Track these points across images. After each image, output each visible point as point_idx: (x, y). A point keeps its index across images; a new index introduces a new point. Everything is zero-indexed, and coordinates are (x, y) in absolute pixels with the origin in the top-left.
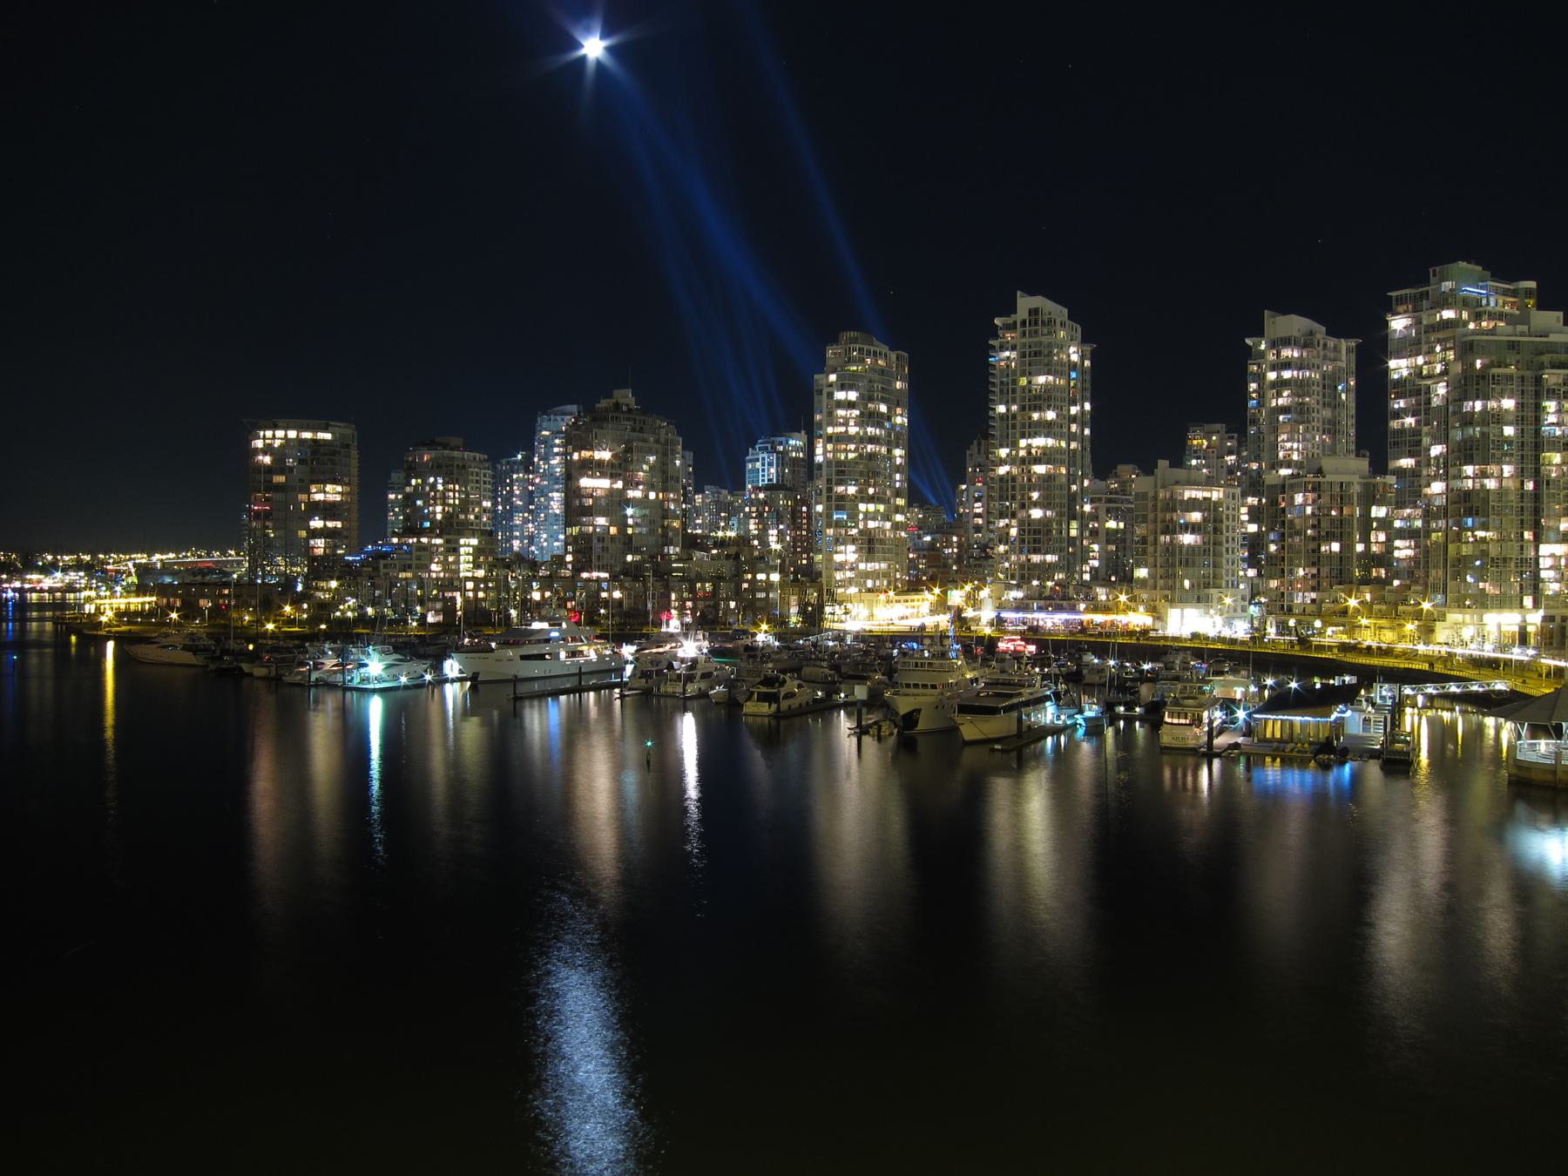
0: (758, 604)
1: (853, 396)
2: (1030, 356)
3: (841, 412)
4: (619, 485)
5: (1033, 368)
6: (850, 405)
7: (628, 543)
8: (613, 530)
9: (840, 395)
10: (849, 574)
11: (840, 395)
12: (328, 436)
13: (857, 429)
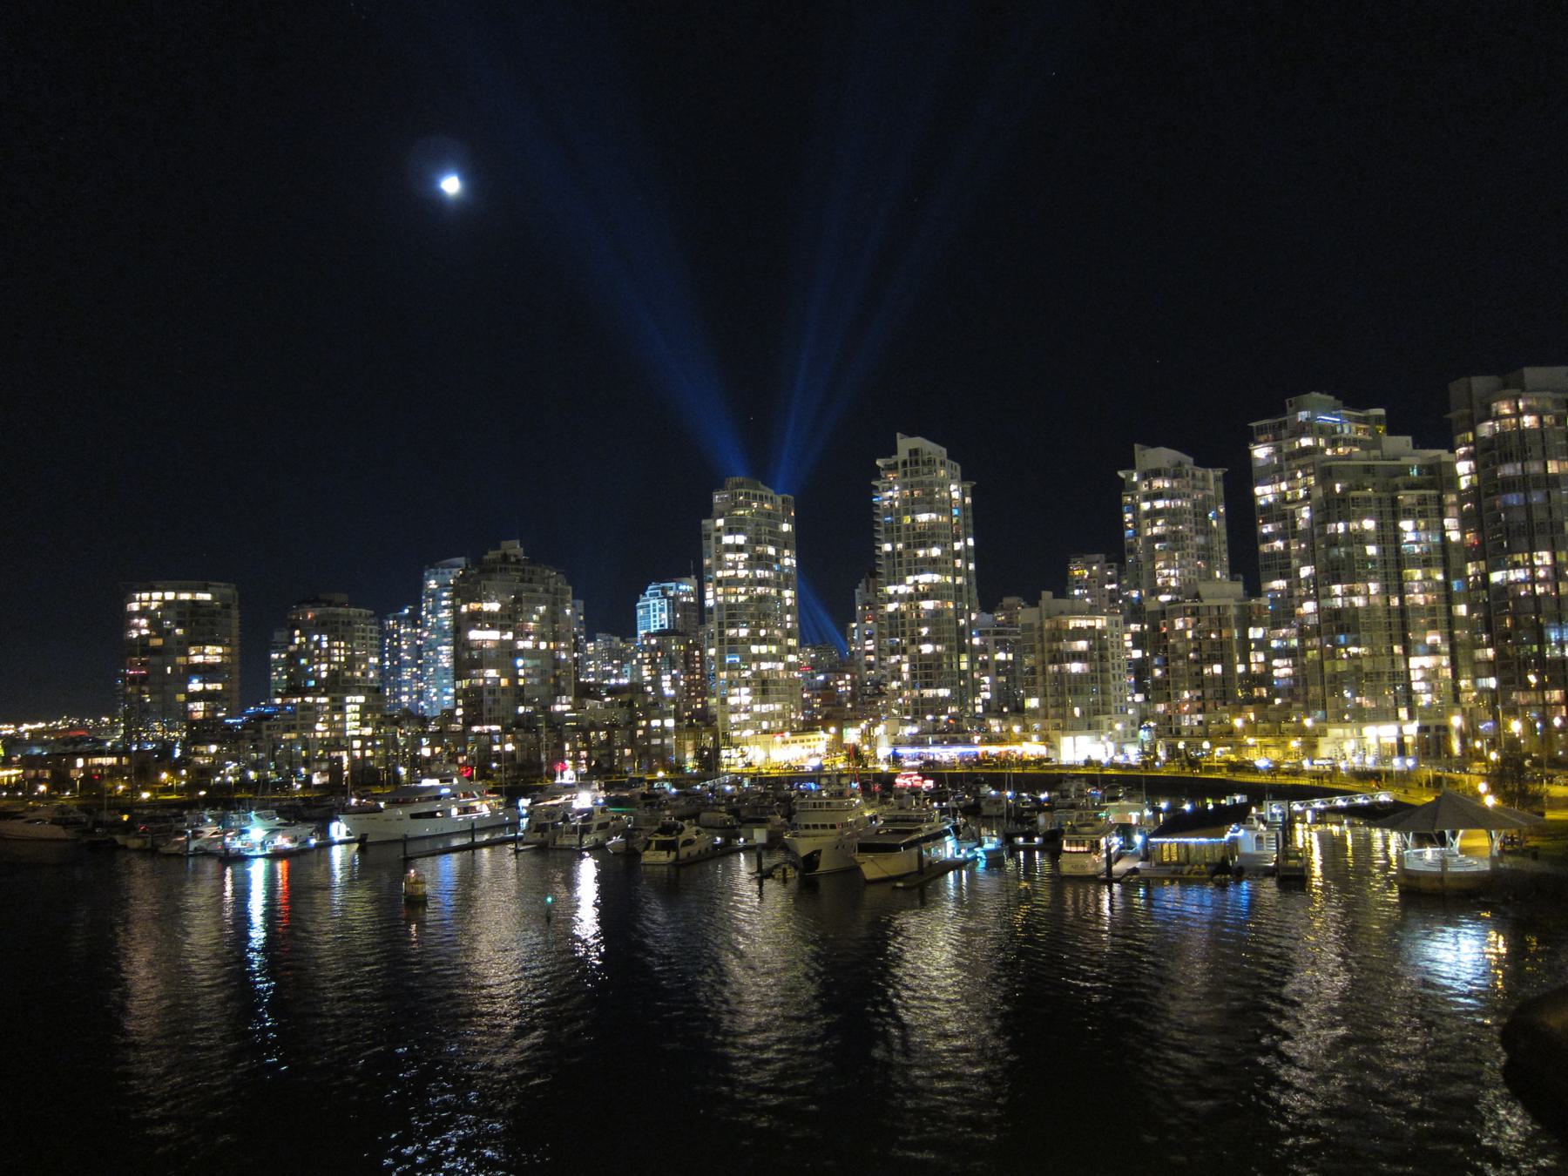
0: (653, 751)
1: (740, 539)
3: (729, 556)
4: (509, 636)
5: (916, 507)
6: (739, 549)
7: (519, 695)
8: (504, 682)
9: (728, 540)
10: (745, 717)
11: (728, 540)
12: (207, 597)
13: (746, 572)
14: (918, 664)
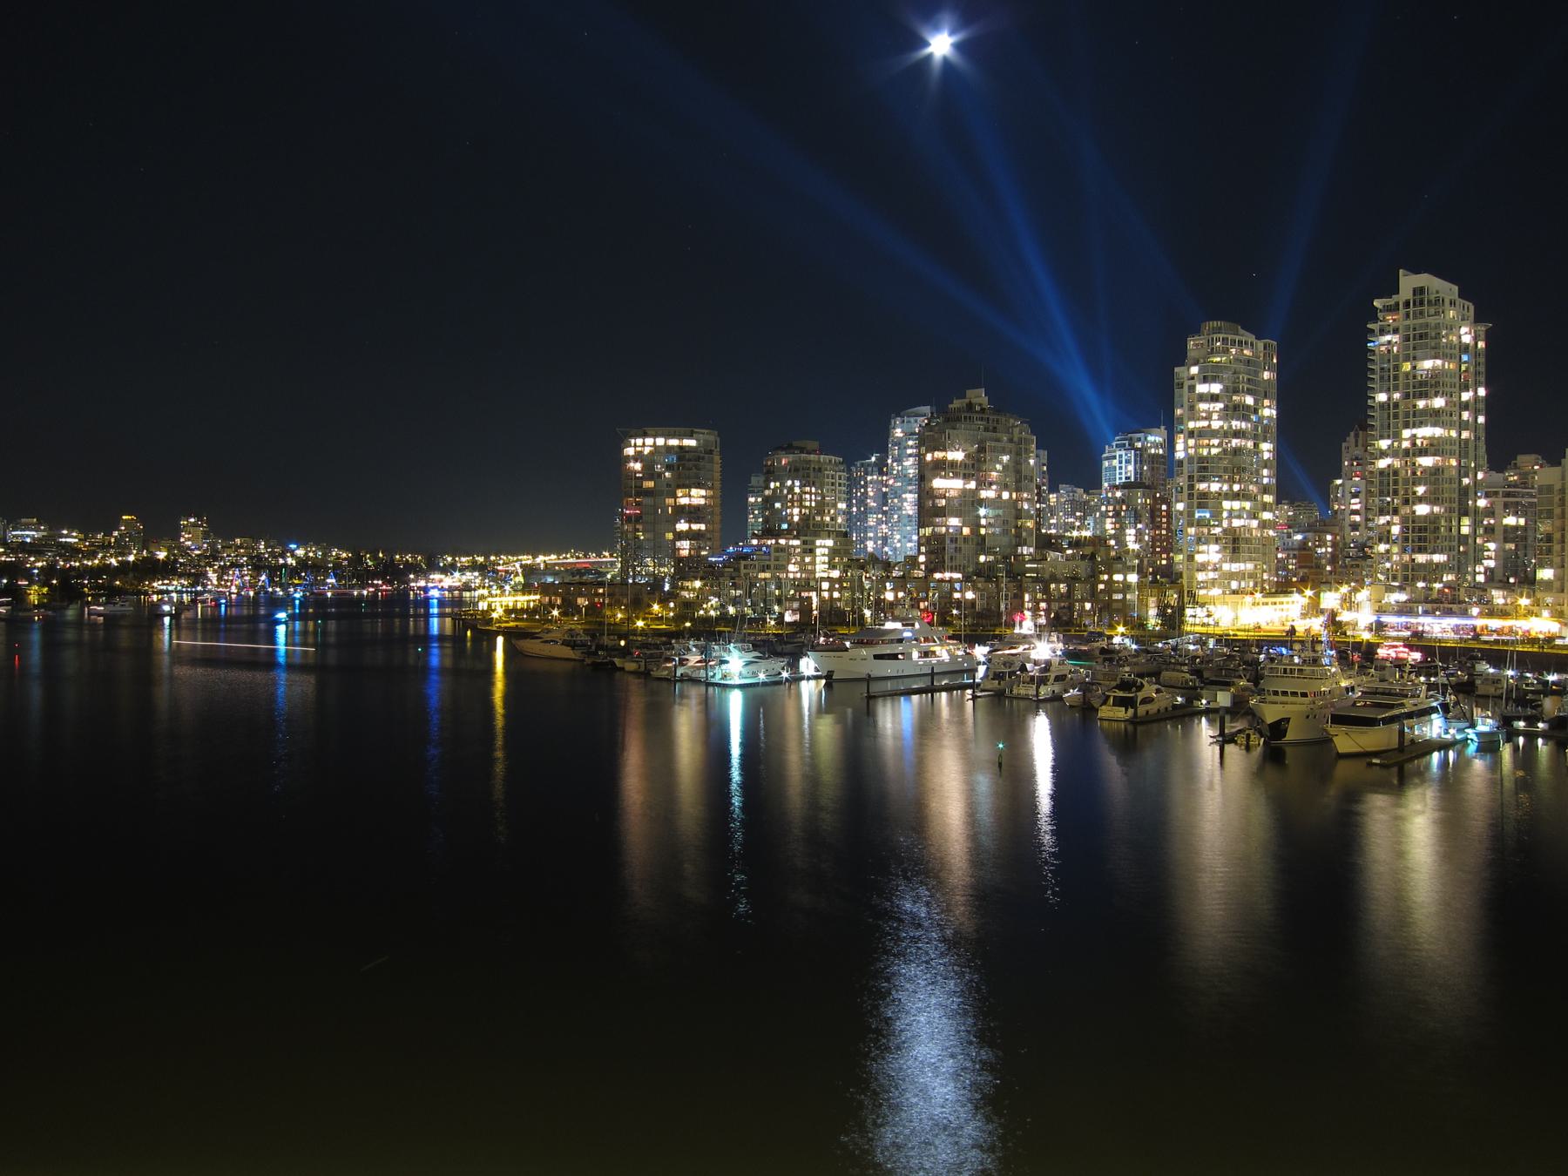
0: (1115, 606)
1: (1216, 388)
2: (1414, 339)
3: (1203, 406)
4: (972, 485)
5: (1419, 353)
6: (1214, 398)
7: (981, 544)
8: (966, 531)
9: (1202, 388)
10: (1211, 575)
11: (1202, 388)
12: (692, 443)
13: (1221, 423)
14: (1410, 525)
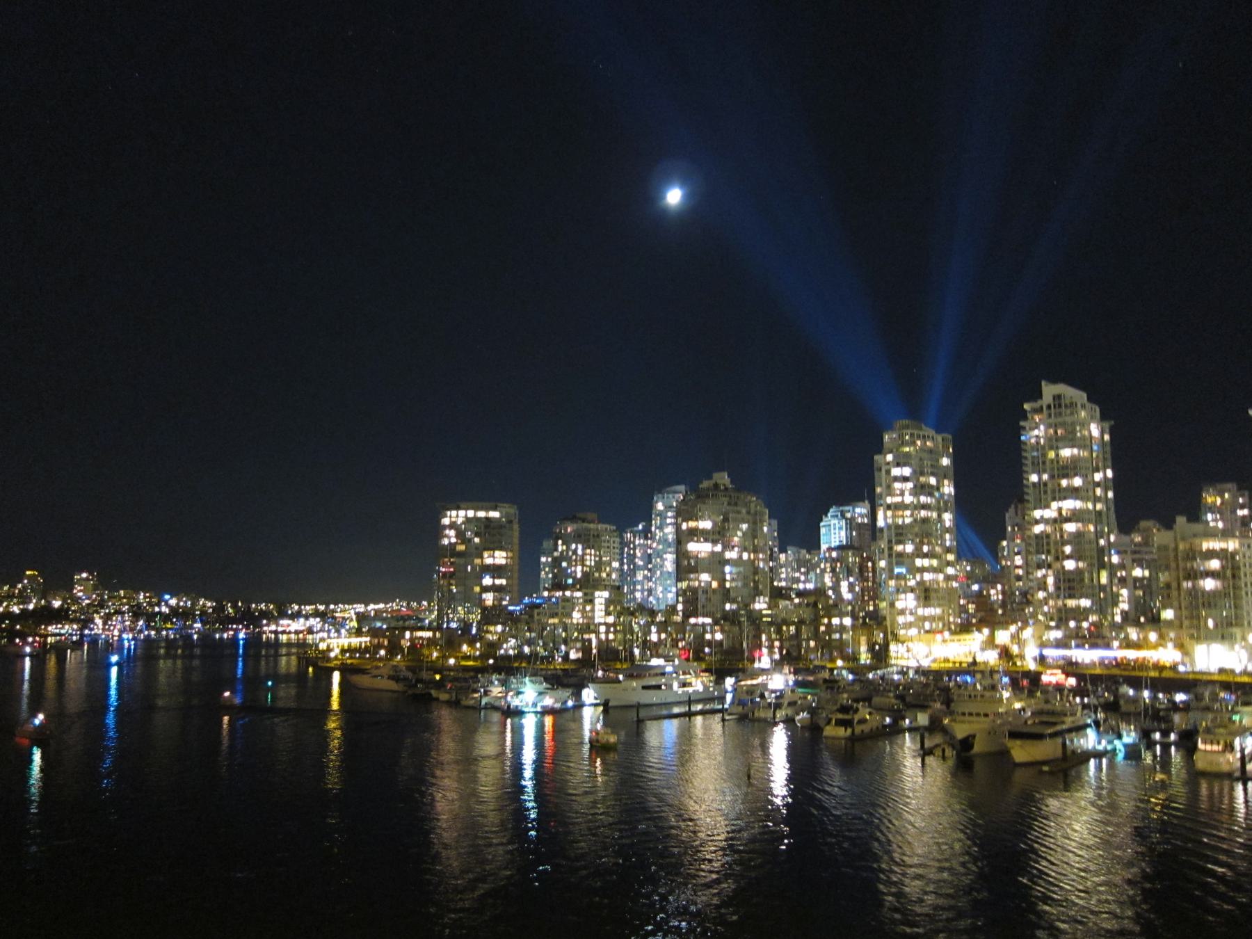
0: (834, 644)
3: (897, 485)
4: (719, 548)
5: (1060, 444)
6: (905, 479)
7: (726, 595)
9: (896, 472)
10: (910, 619)
11: (896, 472)
12: (495, 514)
